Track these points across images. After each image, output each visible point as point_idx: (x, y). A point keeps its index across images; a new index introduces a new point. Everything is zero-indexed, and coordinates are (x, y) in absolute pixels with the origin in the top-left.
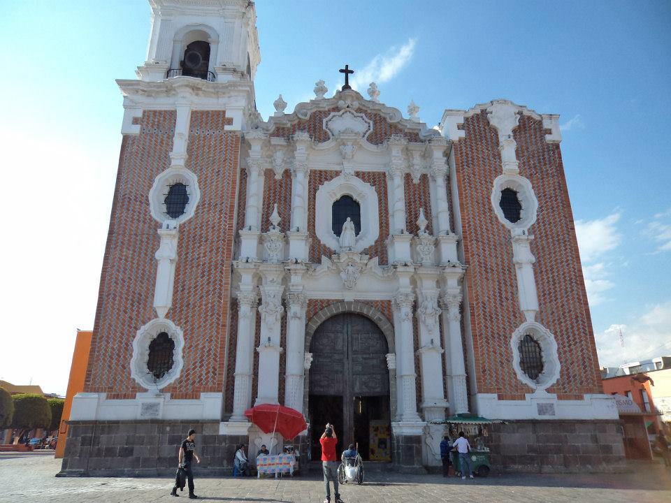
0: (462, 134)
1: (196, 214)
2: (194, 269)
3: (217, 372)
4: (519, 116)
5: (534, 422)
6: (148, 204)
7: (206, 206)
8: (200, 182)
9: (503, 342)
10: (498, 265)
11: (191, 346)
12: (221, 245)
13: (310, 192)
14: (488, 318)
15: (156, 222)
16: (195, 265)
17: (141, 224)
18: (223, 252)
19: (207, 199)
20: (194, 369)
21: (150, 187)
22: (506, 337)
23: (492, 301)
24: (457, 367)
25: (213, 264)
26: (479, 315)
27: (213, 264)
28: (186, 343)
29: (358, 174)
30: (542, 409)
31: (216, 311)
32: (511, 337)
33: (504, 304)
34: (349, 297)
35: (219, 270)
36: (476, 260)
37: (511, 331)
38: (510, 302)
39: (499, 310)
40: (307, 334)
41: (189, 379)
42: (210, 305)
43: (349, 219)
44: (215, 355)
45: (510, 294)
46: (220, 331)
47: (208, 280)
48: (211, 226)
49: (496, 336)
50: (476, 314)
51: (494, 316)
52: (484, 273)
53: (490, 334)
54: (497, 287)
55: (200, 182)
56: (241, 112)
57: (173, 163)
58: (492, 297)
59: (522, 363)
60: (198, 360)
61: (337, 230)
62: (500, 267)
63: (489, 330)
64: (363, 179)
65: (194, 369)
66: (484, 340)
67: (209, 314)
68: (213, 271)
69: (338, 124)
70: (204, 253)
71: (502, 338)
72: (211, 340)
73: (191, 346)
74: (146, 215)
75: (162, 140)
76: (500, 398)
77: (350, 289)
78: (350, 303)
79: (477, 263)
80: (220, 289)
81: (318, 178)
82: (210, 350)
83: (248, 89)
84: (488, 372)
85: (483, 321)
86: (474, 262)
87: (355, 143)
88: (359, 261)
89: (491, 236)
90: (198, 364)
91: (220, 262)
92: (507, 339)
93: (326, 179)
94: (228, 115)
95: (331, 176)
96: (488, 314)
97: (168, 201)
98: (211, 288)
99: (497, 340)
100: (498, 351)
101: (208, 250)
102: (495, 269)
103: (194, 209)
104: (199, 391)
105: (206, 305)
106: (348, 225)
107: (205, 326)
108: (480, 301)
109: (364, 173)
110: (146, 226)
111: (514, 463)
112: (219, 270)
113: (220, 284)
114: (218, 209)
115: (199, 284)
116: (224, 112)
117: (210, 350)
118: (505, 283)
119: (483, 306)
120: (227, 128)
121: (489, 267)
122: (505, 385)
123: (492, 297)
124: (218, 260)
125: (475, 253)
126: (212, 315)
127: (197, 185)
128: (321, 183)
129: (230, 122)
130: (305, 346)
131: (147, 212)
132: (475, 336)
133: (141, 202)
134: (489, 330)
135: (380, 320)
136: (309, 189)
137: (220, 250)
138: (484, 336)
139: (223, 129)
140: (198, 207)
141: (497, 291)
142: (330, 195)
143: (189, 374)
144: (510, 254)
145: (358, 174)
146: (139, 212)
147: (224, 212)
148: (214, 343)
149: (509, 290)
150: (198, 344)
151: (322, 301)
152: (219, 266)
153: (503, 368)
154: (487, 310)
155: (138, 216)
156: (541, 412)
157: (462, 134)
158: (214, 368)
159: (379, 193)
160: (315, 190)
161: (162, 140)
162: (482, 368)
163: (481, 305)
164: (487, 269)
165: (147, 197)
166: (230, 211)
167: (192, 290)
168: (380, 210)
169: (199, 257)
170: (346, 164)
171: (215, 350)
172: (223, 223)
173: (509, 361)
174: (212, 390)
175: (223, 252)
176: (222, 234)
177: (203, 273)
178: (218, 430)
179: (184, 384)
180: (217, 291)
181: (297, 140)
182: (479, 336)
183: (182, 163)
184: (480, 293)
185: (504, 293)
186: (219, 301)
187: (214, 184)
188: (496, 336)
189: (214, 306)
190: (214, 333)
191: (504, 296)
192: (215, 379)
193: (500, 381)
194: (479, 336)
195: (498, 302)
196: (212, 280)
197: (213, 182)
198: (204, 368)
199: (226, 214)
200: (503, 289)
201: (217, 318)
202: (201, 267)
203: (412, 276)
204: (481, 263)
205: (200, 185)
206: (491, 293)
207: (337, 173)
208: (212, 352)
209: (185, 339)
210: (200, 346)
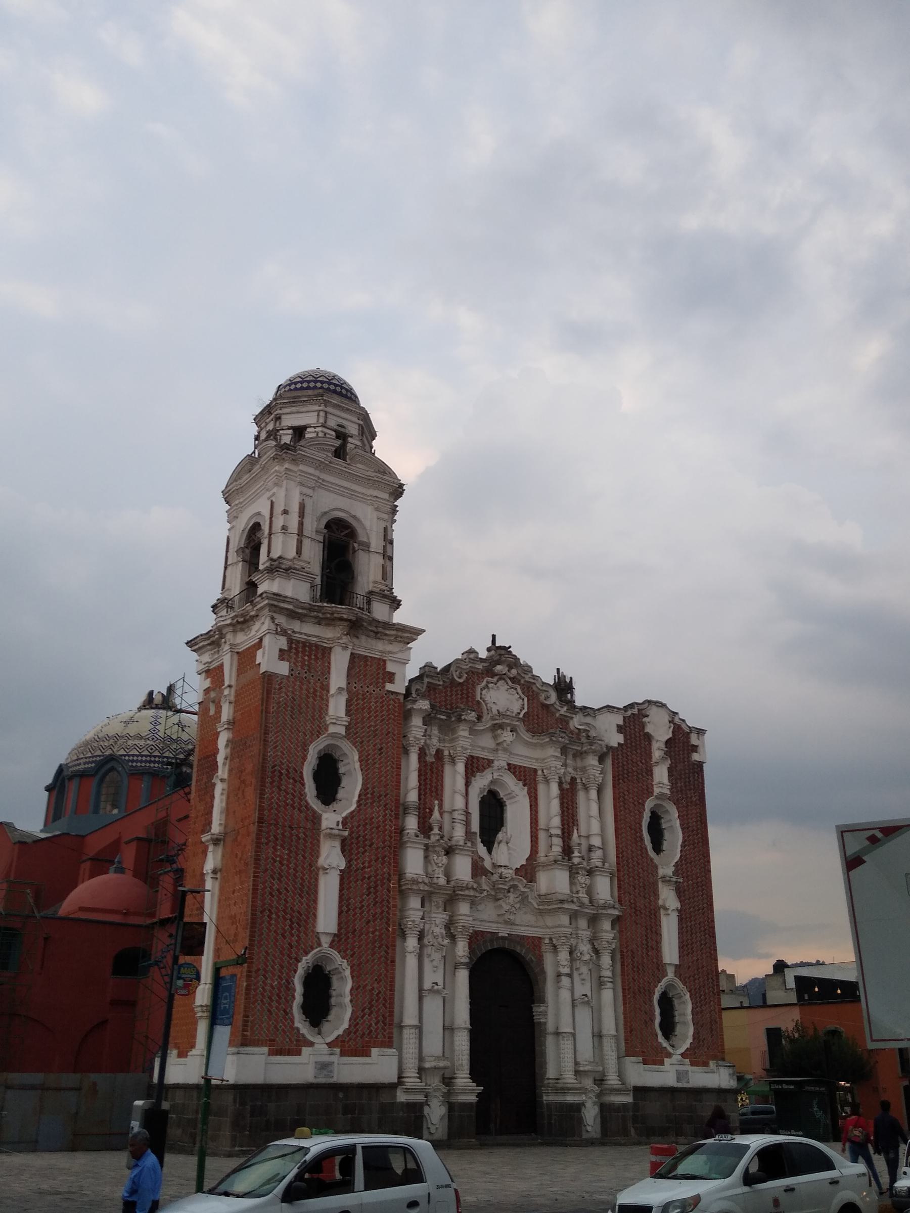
1: (358, 806)
2: (359, 882)
5: (672, 1090)
6: (303, 785)
7: (369, 796)
15: (314, 812)
16: (360, 877)
17: (296, 812)
21: (304, 758)
29: (512, 768)
30: (680, 1076)
34: (504, 932)
48: (375, 825)
57: (332, 729)
64: (514, 774)
68: (379, 888)
69: (501, 698)
70: (369, 862)
74: (301, 800)
75: (315, 691)
76: (645, 1062)
77: (508, 923)
78: (503, 938)
91: (386, 875)
93: (478, 770)
94: (390, 667)
97: (317, 776)
101: (373, 857)
102: (643, 911)
103: (356, 798)
109: (515, 766)
110: (303, 815)
116: (384, 661)
120: (389, 687)
124: (384, 873)
127: (357, 765)
129: (391, 677)
131: (302, 795)
133: (293, 779)
135: (532, 961)
139: (384, 687)
140: (360, 796)
144: (656, 895)
145: (512, 768)
146: (293, 795)
155: (292, 800)
156: (679, 1080)
161: (315, 691)
165: (302, 773)
169: (364, 867)
170: (501, 754)
173: (652, 1020)
176: (387, 838)
181: (465, 720)
183: (342, 731)
187: (377, 765)
202: (366, 880)
205: (361, 766)
207: (490, 763)
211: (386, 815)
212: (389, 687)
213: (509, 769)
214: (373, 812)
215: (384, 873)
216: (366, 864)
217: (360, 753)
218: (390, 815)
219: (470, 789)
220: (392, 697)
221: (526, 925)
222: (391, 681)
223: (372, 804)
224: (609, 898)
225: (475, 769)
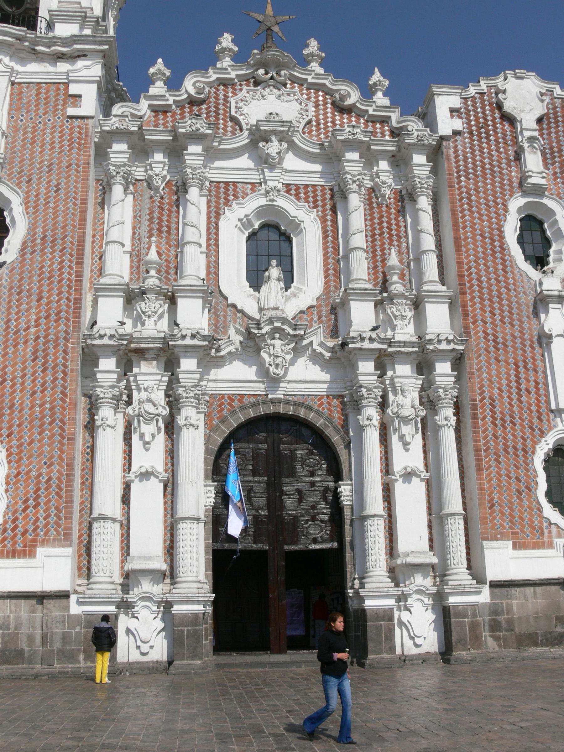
0: (458, 124)
3: (63, 515)
4: (547, 99)
8: (28, 202)
9: (521, 458)
10: (515, 337)
11: (19, 473)
12: (64, 307)
13: (209, 218)
14: (499, 422)
18: (68, 320)
19: (39, 230)
20: (24, 510)
22: (526, 452)
23: (505, 394)
24: (453, 501)
25: (52, 337)
26: (485, 417)
27: (52, 337)
28: (10, 468)
31: (58, 416)
32: (534, 453)
33: (524, 399)
35: (61, 348)
36: (480, 328)
37: (535, 443)
38: (533, 395)
39: (516, 409)
40: (207, 451)
41: (16, 527)
42: (48, 406)
43: (274, 262)
44: (58, 487)
45: (532, 384)
46: (65, 448)
47: (43, 365)
49: (511, 450)
50: (480, 416)
51: (508, 418)
52: (492, 349)
53: (501, 447)
54: (513, 372)
55: (26, 203)
56: (95, 86)
58: (505, 387)
59: (548, 494)
60: (31, 495)
61: (256, 279)
62: (518, 340)
63: (501, 441)
65: (24, 510)
66: (493, 457)
67: (47, 420)
68: (51, 350)
70: (36, 321)
71: (520, 453)
72: (52, 464)
73: (19, 473)
79: (481, 334)
80: (63, 379)
81: (222, 195)
82: (50, 479)
83: (106, 47)
84: (497, 508)
85: (490, 426)
86: (478, 332)
87: (283, 137)
88: (292, 332)
89: (503, 290)
90: (31, 502)
92: (528, 452)
93: (236, 197)
94: (73, 89)
95: (243, 192)
96: (498, 415)
98: (50, 378)
99: (512, 456)
100: (513, 474)
101: (43, 314)
102: (509, 343)
104: (35, 546)
105: (41, 406)
106: (275, 272)
107: (40, 441)
108: (487, 395)
111: (536, 644)
112: (61, 348)
113: (64, 372)
114: (58, 247)
115: (29, 371)
116: (67, 85)
117: (50, 479)
118: (525, 367)
119: (491, 404)
121: (500, 340)
122: (524, 527)
123: (505, 387)
125: (479, 317)
126: (50, 424)
128: (227, 203)
130: (206, 471)
132: (477, 451)
134: (501, 441)
136: (209, 213)
137: (63, 314)
138: (492, 450)
140: (24, 243)
141: (513, 378)
142: (243, 224)
143: (16, 519)
147: (68, 250)
148: (56, 467)
149: (531, 377)
150: (30, 470)
151: (231, 398)
152: (62, 341)
153: (521, 500)
154: (498, 409)
157: (458, 124)
158: (57, 508)
159: (323, 220)
160: (218, 215)
162: (489, 502)
163: (487, 401)
164: (497, 343)
166: (78, 250)
167: (19, 380)
168: (325, 248)
171: (59, 479)
172: (66, 270)
173: (531, 488)
174: (56, 542)
175: (68, 320)
177: (35, 352)
178: (68, 608)
179: (9, 533)
180: (59, 382)
182: (485, 451)
184: (486, 382)
185: (522, 381)
186: (62, 399)
188: (511, 450)
189: (55, 407)
190: (56, 452)
191: (523, 387)
192: (59, 526)
193: (516, 520)
194: (485, 451)
195: (515, 396)
196: (50, 364)
197: (49, 202)
198: (41, 509)
199: (71, 255)
200: (522, 375)
201: (61, 428)
203: (378, 358)
204: (488, 335)
206: (504, 382)
208: (54, 483)
209: (9, 462)
210: (34, 473)
211: (63, 261)
212: (71, 111)
213: (288, 191)
214: (44, 260)
215: (59, 332)
216: (32, 323)
217: (26, 193)
218: (70, 261)
219: (222, 223)
220: (77, 123)
221: (305, 379)
222: (74, 105)
223: (42, 251)
224: (450, 331)
225: (231, 198)
